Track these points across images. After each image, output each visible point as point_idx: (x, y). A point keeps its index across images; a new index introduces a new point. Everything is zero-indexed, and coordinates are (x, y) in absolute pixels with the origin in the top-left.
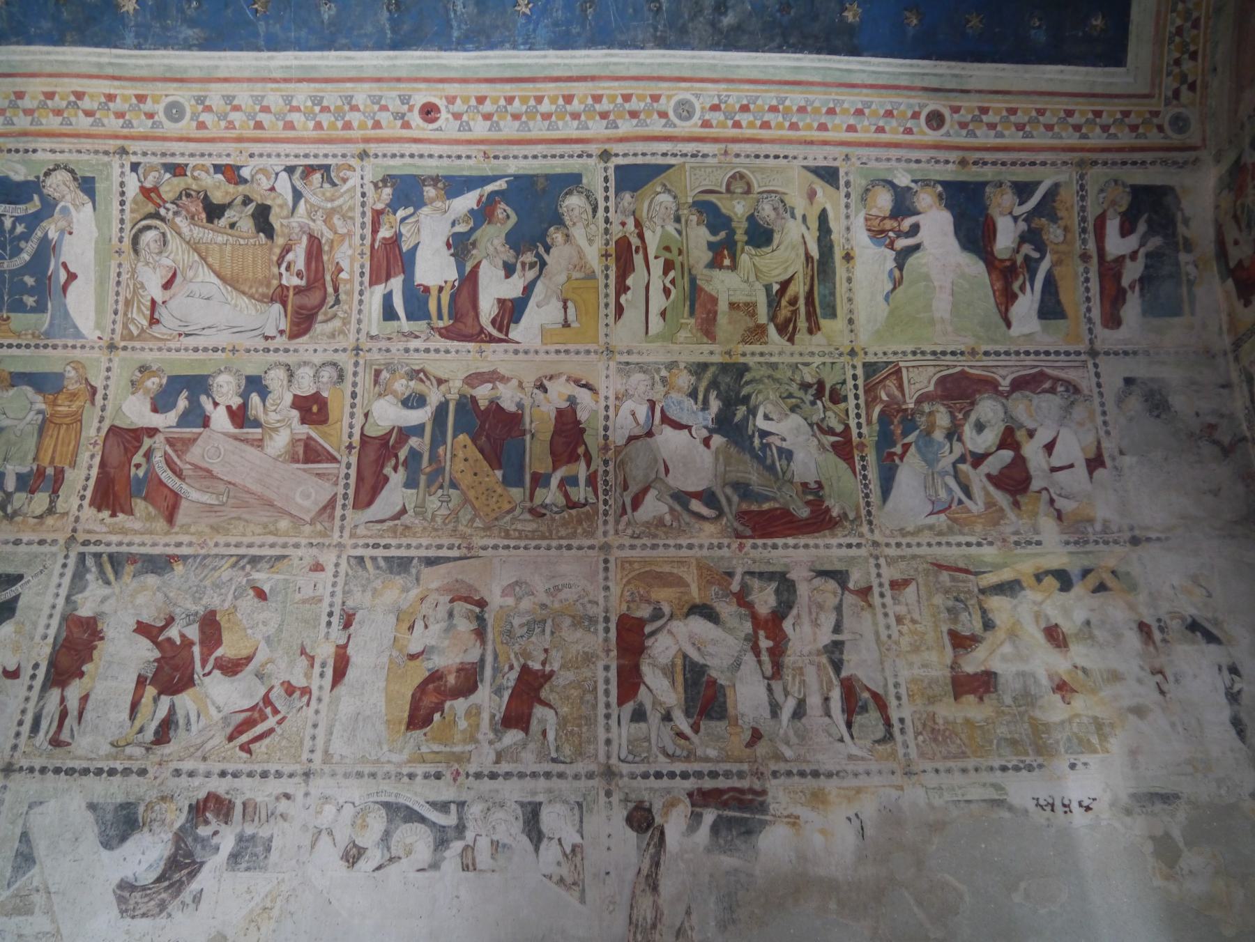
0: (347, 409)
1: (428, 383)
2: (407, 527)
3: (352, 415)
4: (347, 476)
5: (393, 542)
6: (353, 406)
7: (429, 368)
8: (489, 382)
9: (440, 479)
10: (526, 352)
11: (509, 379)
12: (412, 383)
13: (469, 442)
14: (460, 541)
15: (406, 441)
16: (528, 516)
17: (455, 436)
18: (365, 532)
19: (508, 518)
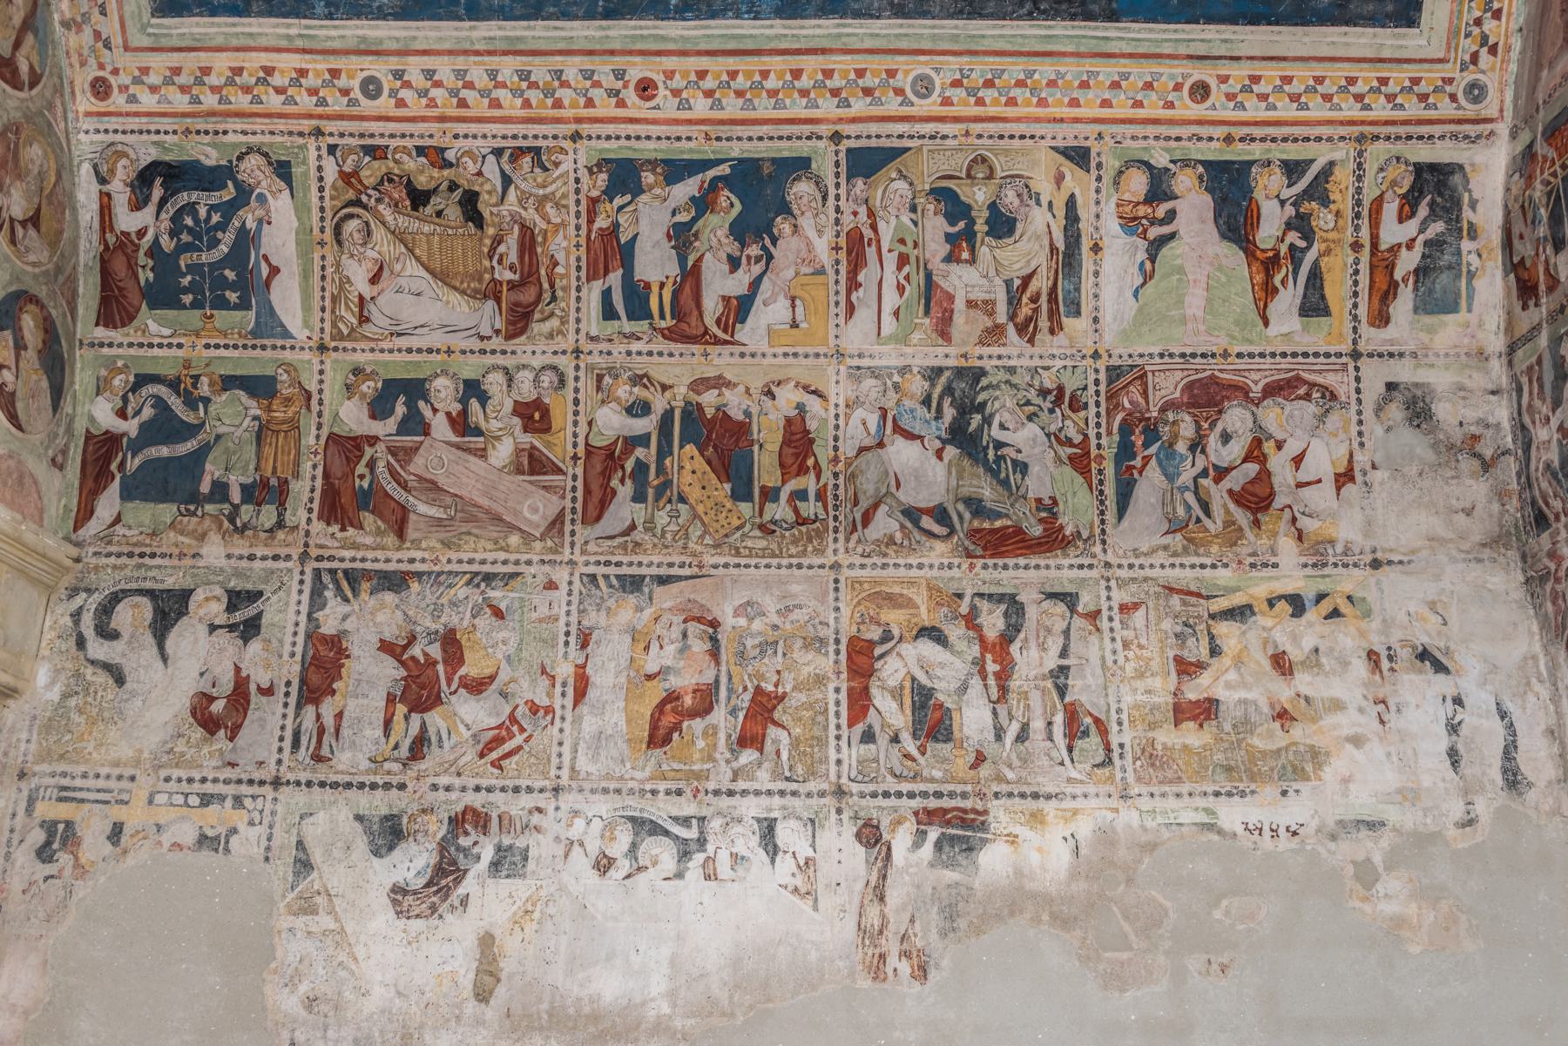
0: (570, 418)
3: (576, 423)
4: (574, 489)
6: (576, 413)
7: (652, 373)
10: (753, 355)
11: (735, 385)
12: (636, 390)
13: (696, 453)
15: (632, 452)
16: (757, 533)
17: (681, 447)
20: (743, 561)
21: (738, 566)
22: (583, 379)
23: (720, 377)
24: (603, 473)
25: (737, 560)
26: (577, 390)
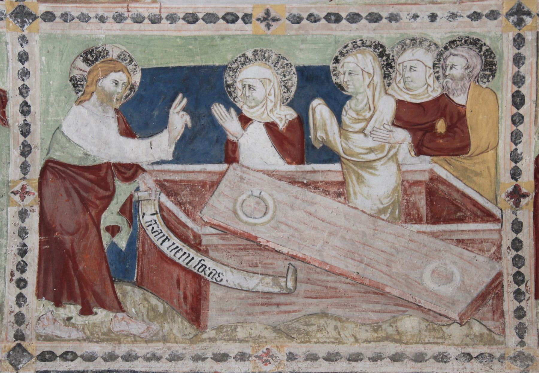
4: (517, 244)
26: (518, 80)
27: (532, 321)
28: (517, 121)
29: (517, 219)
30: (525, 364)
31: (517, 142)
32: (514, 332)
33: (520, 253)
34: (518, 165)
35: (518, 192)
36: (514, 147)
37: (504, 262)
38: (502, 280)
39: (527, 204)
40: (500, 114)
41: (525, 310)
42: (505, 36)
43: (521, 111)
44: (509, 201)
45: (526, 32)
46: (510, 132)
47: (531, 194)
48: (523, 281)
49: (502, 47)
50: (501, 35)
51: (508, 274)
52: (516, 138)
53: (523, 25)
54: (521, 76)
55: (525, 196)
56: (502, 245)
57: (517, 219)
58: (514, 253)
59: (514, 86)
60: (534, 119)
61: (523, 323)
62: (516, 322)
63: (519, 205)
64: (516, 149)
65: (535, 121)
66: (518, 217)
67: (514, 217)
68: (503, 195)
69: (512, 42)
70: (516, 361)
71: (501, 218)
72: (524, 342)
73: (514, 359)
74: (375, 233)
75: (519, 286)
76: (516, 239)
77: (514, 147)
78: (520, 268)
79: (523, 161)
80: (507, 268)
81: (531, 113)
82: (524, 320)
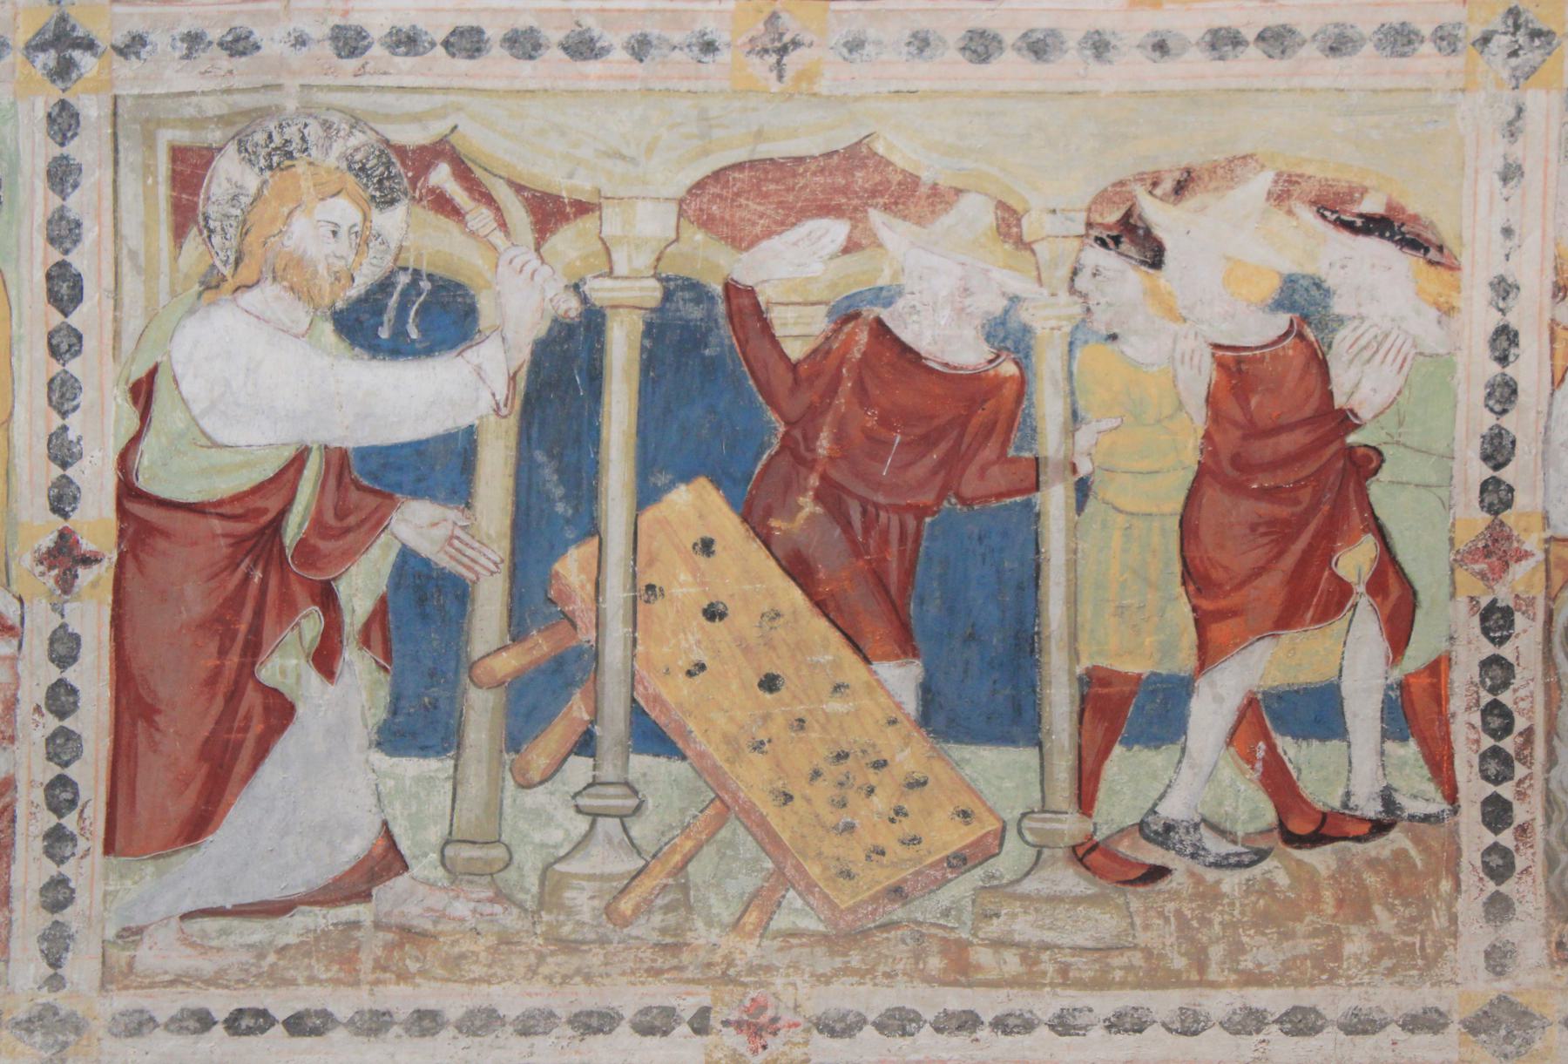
1: (480, 218)
2: (408, 935)
3: (62, 394)
4: (61, 699)
5: (343, 1004)
6: (64, 344)
7: (477, 139)
8: (826, 210)
9: (578, 709)
10: (1039, 47)
11: (940, 198)
12: (392, 222)
13: (726, 523)
14: (703, 997)
15: (376, 523)
16: (1071, 880)
17: (646, 495)
18: (182, 960)
19: (962, 887)
20: (988, 1004)
21: (967, 1022)
22: (95, 178)
23: (856, 156)
24: (219, 624)
25: (955, 1000)
26: (63, 231)
27: (89, 918)
28: (64, 347)
29: (63, 626)
30: (56, 1041)
31: (66, 407)
32: (34, 948)
33: (68, 723)
34: (70, 472)
35: (70, 552)
36: (57, 422)
37: (21, 750)
38: (14, 800)
39: (94, 584)
40: (14, 327)
41: (72, 885)
42: (23, 107)
43: (75, 320)
44: (43, 574)
45: (82, 96)
46: (45, 381)
47: (108, 555)
48: (72, 803)
49: (16, 139)
50: (14, 104)
51: (31, 783)
52: (62, 396)
53: (74, 76)
54: (69, 222)
55: (88, 560)
56: (17, 700)
57: (63, 626)
58: (52, 723)
59: (50, 248)
60: (111, 342)
61: (63, 924)
62: (45, 919)
63: (72, 585)
64: (65, 428)
65: (114, 348)
66: (66, 620)
67: (56, 621)
68: (28, 560)
69: (44, 124)
70: (30, 1032)
71: (18, 624)
72: (63, 978)
73: (28, 1025)
74: (386, 252)
75: (60, 816)
76: (61, 683)
77: (57, 422)
78: (66, 764)
79: (85, 461)
80: (29, 768)
81: (101, 326)
82: (67, 915)
